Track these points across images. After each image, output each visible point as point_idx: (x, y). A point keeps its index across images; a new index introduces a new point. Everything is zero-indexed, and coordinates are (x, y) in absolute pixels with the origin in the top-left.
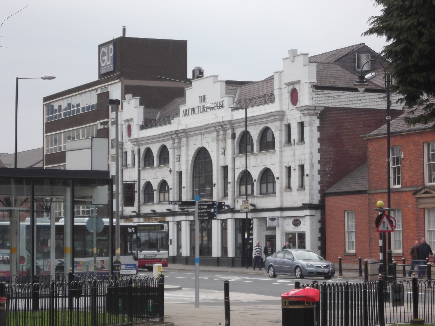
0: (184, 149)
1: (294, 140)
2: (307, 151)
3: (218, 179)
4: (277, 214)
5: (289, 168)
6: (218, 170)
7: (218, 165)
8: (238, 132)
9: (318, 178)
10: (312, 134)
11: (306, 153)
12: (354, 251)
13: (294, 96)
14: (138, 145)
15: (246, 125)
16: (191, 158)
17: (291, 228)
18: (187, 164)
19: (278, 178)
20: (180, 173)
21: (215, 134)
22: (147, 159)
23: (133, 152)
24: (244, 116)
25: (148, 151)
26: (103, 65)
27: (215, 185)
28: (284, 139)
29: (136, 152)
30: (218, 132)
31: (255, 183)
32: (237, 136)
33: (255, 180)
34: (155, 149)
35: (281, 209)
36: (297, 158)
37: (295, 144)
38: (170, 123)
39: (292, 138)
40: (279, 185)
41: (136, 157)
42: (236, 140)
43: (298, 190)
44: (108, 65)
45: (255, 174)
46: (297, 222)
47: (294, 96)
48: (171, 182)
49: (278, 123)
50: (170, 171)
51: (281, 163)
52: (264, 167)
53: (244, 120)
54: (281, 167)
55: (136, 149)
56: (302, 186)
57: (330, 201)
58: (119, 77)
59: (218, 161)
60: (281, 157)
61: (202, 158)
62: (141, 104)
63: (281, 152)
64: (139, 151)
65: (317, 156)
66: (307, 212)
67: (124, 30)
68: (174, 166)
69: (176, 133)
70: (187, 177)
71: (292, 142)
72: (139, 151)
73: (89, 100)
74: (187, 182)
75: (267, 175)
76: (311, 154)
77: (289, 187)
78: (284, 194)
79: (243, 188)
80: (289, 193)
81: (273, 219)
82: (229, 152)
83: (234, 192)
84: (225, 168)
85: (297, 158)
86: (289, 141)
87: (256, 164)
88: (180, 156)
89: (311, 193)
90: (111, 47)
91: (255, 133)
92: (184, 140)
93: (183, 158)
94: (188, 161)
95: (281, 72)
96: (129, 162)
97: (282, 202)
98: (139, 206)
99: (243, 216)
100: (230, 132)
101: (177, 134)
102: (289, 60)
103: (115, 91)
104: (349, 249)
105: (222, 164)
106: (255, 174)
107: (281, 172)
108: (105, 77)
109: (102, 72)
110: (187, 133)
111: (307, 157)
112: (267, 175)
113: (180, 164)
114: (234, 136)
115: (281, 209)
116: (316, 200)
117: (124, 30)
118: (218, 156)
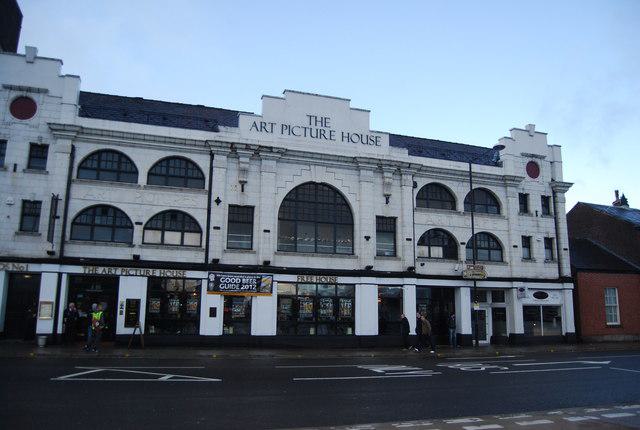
8: (422, 182)
13: (533, 170)
14: (75, 139)
17: (531, 300)
33: (462, 244)
38: (217, 131)
47: (533, 170)
80: (529, 264)
85: (541, 229)
98: (63, 242)
114: (415, 185)
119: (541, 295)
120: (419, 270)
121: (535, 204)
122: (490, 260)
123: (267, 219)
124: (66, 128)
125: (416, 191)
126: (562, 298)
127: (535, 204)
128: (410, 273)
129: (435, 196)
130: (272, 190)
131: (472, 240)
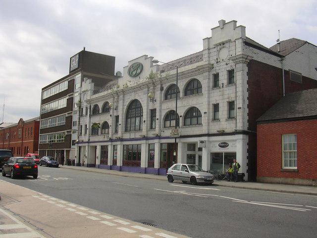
0: (121, 102)
1: (223, 84)
2: (240, 89)
3: (147, 118)
4: (205, 139)
5: (216, 107)
6: (147, 112)
7: (147, 109)
9: (247, 110)
10: (241, 78)
11: (239, 92)
12: (296, 168)
15: (177, 79)
16: (125, 107)
18: (123, 111)
19: (205, 113)
20: (117, 117)
21: (147, 89)
22: (95, 111)
23: (87, 108)
24: (176, 73)
25: (96, 106)
26: (72, 66)
27: (145, 121)
28: (211, 84)
29: (89, 108)
30: (148, 88)
31: (181, 119)
32: (165, 88)
33: (181, 116)
34: (100, 105)
35: (209, 135)
36: (226, 97)
37: (224, 86)
39: (220, 83)
40: (204, 119)
41: (89, 110)
42: (163, 92)
43: (226, 120)
44: (75, 65)
45: (181, 112)
46: (224, 145)
48: (110, 122)
49: (207, 74)
50: (111, 116)
51: (209, 102)
52: (188, 107)
53: (176, 75)
54: (209, 105)
55: (88, 106)
56: (230, 117)
57: (262, 129)
58: (81, 70)
59: (148, 106)
60: (209, 97)
61: (134, 108)
62: (92, 82)
63: (209, 94)
64: (90, 106)
65: (247, 95)
66: (241, 136)
67: (84, 49)
68: (113, 113)
69: (117, 93)
70: (123, 119)
71: (220, 85)
72: (90, 106)
73: (64, 86)
74: (122, 122)
75: (193, 114)
76: (243, 91)
77: (215, 119)
78: (211, 124)
79: (168, 123)
80: (215, 123)
81: (202, 142)
82: (158, 99)
83: (160, 125)
84: (153, 112)
86: (216, 84)
87: (182, 106)
88: (117, 107)
89: (241, 121)
90: (78, 56)
91: (181, 85)
92: (121, 97)
93: (120, 107)
94: (123, 108)
95: (209, 38)
96: (84, 113)
97: (209, 130)
99: (173, 141)
100: (159, 86)
101: (117, 94)
102: (219, 28)
103: (78, 77)
104: (285, 166)
105: (151, 107)
106: (181, 112)
107: (209, 108)
108: (73, 72)
109: (71, 70)
110: (124, 92)
111: (240, 94)
112: (193, 114)
113: (117, 112)
114: (162, 89)
115: (209, 135)
116: (246, 129)
117: (84, 49)
118: (148, 103)
119: (224, 145)
120: (163, 135)
121: (223, 79)
122: (197, 124)
123: (121, 120)
124: (184, 73)
125: (163, 92)
126: (238, 147)
127: (223, 79)
128: (159, 137)
129: (171, 92)
130: (122, 107)
131: (177, 114)
